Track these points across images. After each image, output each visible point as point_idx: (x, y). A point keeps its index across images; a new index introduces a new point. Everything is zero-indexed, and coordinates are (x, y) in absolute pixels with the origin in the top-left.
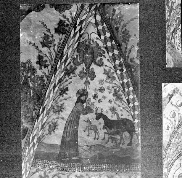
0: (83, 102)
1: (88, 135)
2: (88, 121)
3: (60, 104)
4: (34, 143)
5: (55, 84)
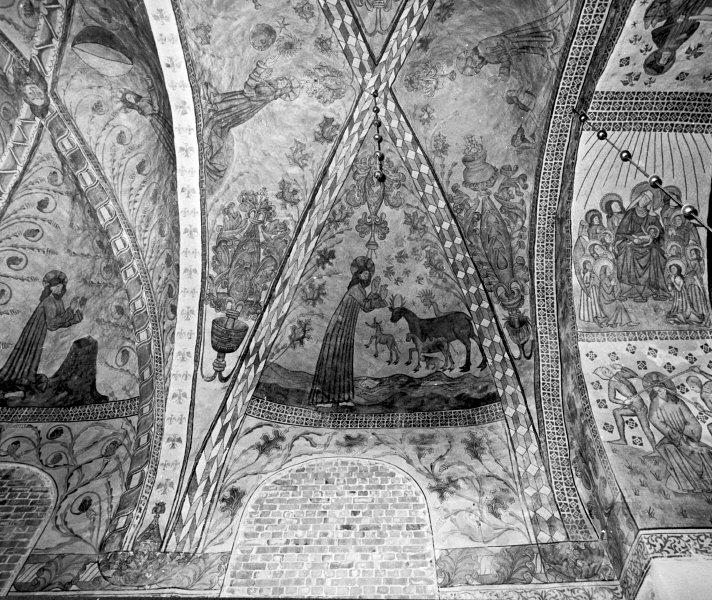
0: (365, 283)
1: (376, 356)
2: (376, 325)
3: (317, 282)
4: (258, 356)
5: (309, 234)
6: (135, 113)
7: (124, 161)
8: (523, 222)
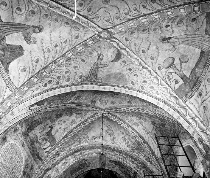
6: (98, 57)
7: (84, 55)
8: (79, 145)
